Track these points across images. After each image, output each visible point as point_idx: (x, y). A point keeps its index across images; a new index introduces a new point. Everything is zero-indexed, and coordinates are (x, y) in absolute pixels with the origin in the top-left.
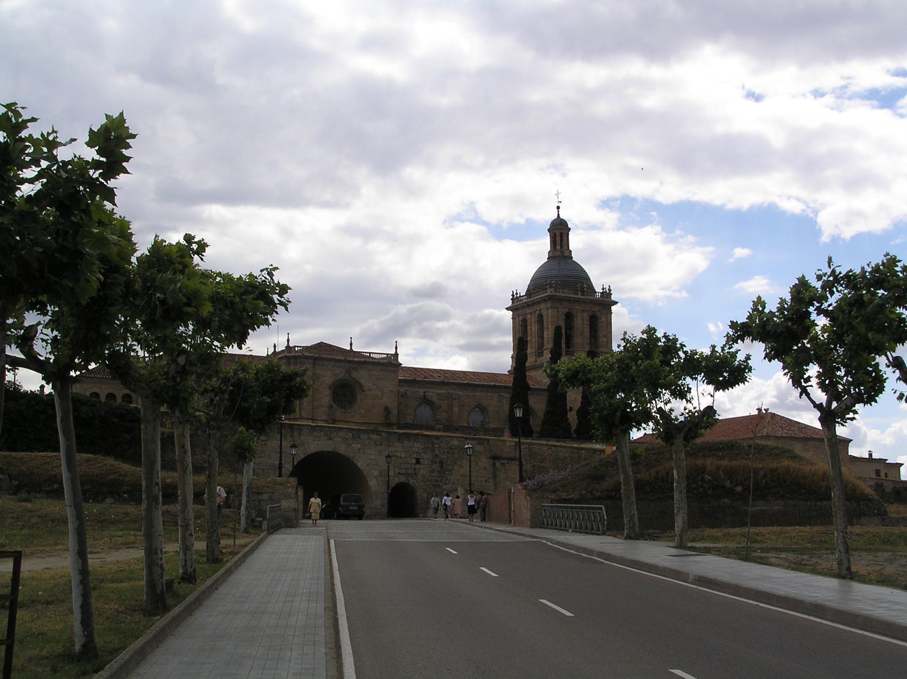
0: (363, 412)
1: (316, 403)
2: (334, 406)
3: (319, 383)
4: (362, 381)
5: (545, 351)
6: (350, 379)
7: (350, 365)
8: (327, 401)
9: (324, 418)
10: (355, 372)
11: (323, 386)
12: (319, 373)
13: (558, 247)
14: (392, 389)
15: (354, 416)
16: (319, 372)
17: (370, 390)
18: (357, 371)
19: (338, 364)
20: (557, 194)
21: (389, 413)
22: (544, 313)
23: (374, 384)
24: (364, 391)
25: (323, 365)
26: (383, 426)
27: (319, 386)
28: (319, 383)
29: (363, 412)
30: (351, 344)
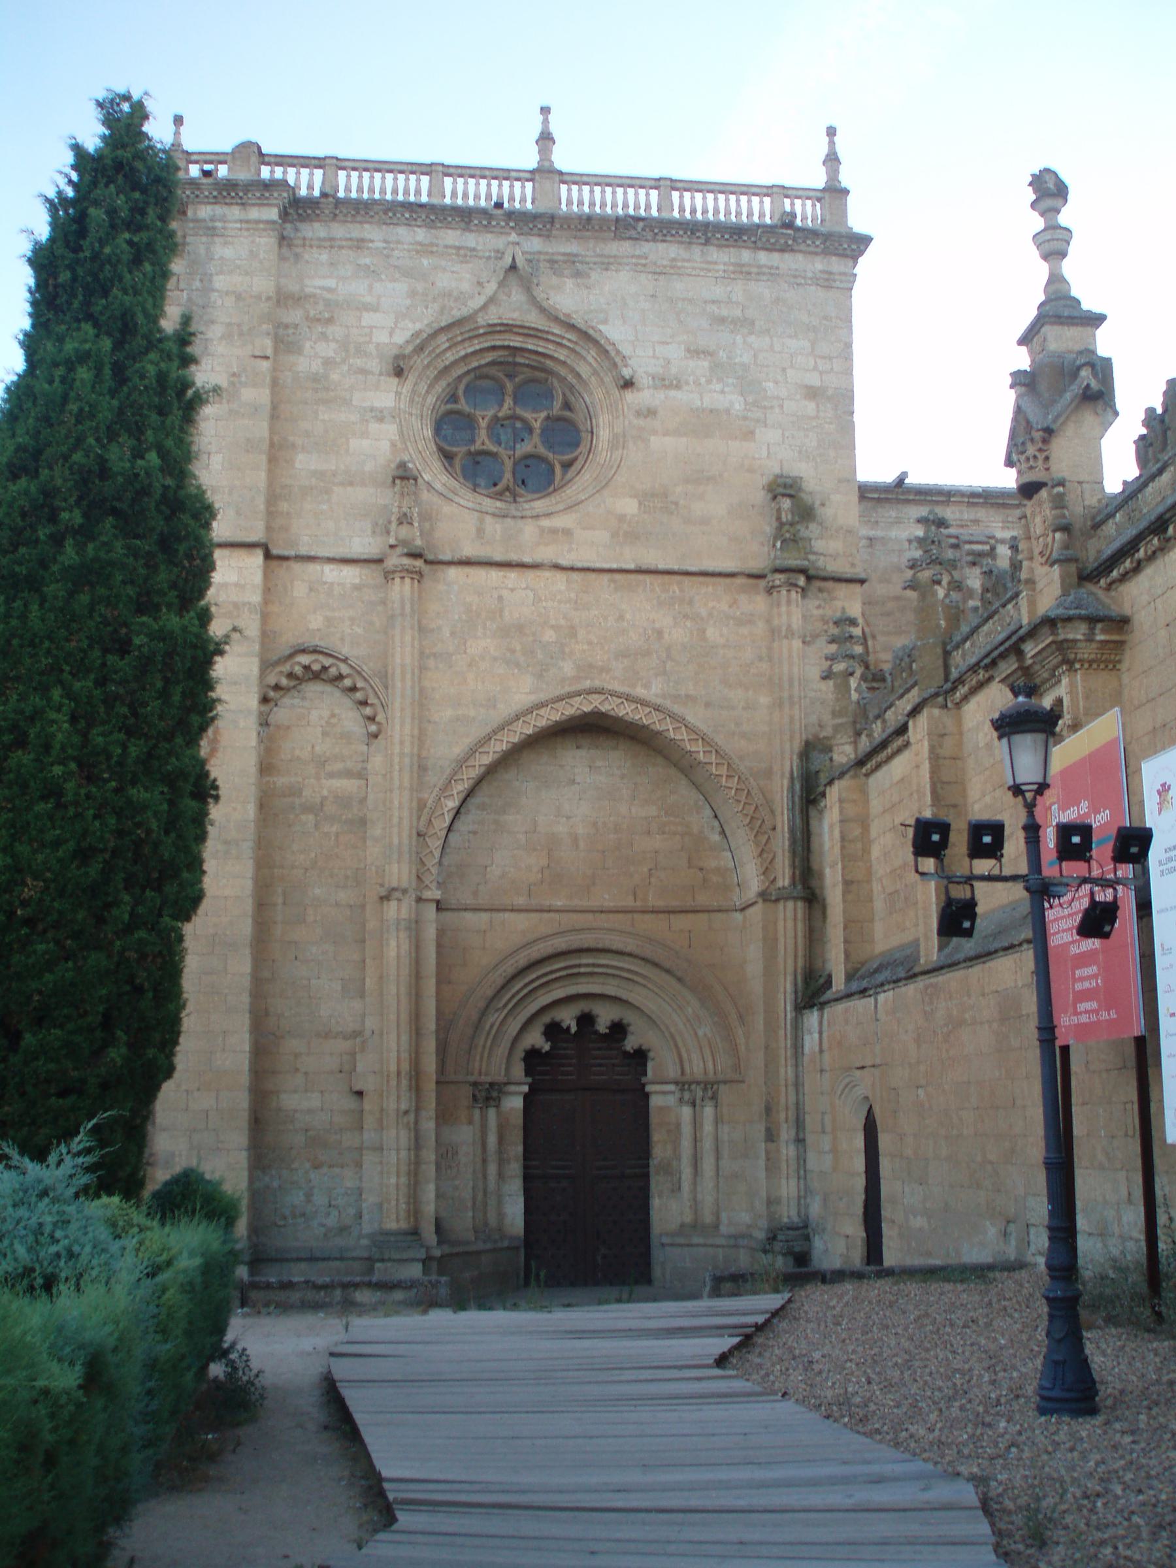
0: (629, 506)
1: (305, 463)
2: (434, 473)
3: (328, 350)
4: (614, 332)
6: (533, 319)
7: (534, 244)
8: (385, 446)
9: (363, 544)
10: (569, 283)
11: (359, 362)
12: (330, 290)
14: (814, 380)
15: (567, 532)
16: (331, 283)
17: (665, 382)
18: (578, 274)
19: (451, 237)
21: (806, 513)
23: (695, 352)
24: (628, 384)
25: (359, 244)
26: (770, 590)
27: (328, 362)
28: (328, 350)
29: (629, 506)
30: (546, 139)
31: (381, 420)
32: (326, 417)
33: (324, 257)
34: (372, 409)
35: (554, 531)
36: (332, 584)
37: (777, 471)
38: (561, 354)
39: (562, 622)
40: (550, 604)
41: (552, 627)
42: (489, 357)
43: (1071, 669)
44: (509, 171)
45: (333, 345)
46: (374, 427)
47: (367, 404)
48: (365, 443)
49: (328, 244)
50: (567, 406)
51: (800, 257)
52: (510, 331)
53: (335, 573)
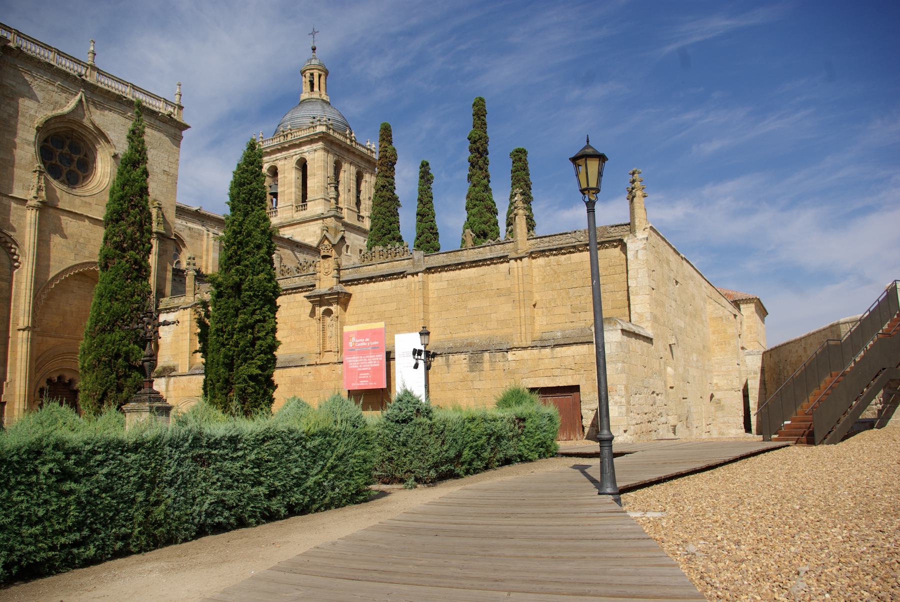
5: (309, 204)
12: (13, 86)
13: (316, 89)
14: (166, 169)
15: (90, 204)
16: (14, 84)
20: (314, 33)
22: (308, 157)
31: (29, 145)
32: (8, 138)
33: (12, 71)
34: (26, 140)
35: (86, 203)
36: (6, 205)
37: (154, 198)
38: (90, 137)
39: (86, 236)
40: (83, 229)
41: (83, 237)
42: (63, 130)
43: (338, 304)
44: (80, 61)
45: (13, 109)
46: (26, 147)
47: (24, 137)
48: (22, 152)
49: (13, 67)
50: (85, 156)
51: (168, 126)
52: (76, 124)
53: (7, 201)
